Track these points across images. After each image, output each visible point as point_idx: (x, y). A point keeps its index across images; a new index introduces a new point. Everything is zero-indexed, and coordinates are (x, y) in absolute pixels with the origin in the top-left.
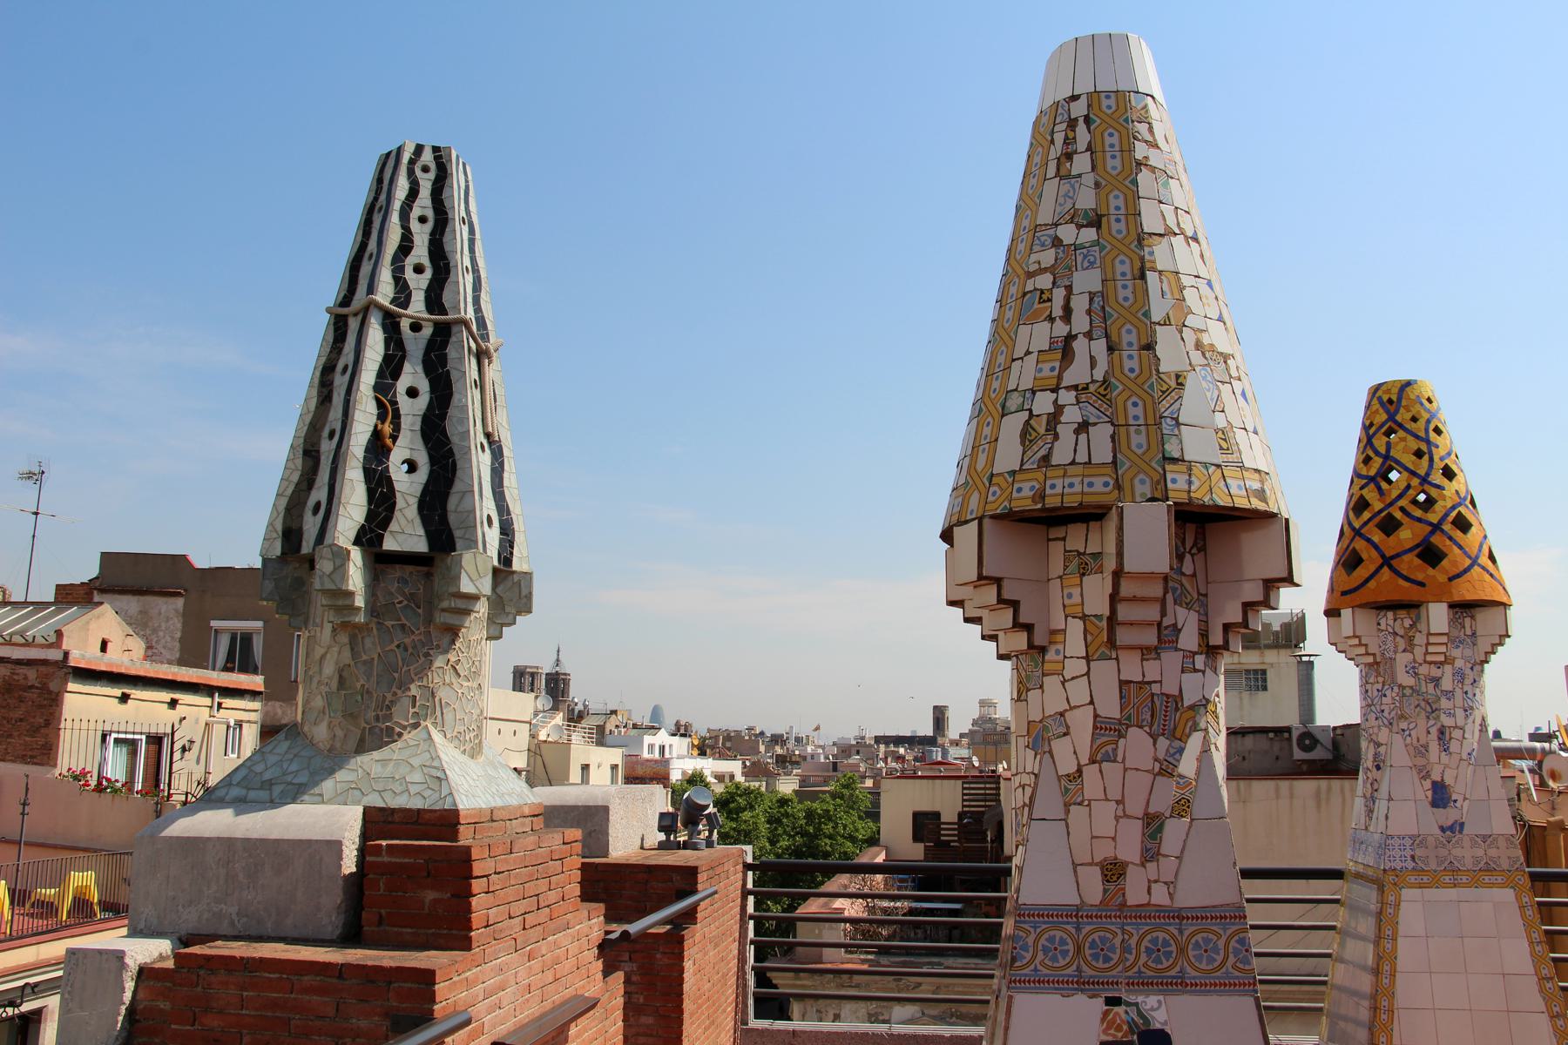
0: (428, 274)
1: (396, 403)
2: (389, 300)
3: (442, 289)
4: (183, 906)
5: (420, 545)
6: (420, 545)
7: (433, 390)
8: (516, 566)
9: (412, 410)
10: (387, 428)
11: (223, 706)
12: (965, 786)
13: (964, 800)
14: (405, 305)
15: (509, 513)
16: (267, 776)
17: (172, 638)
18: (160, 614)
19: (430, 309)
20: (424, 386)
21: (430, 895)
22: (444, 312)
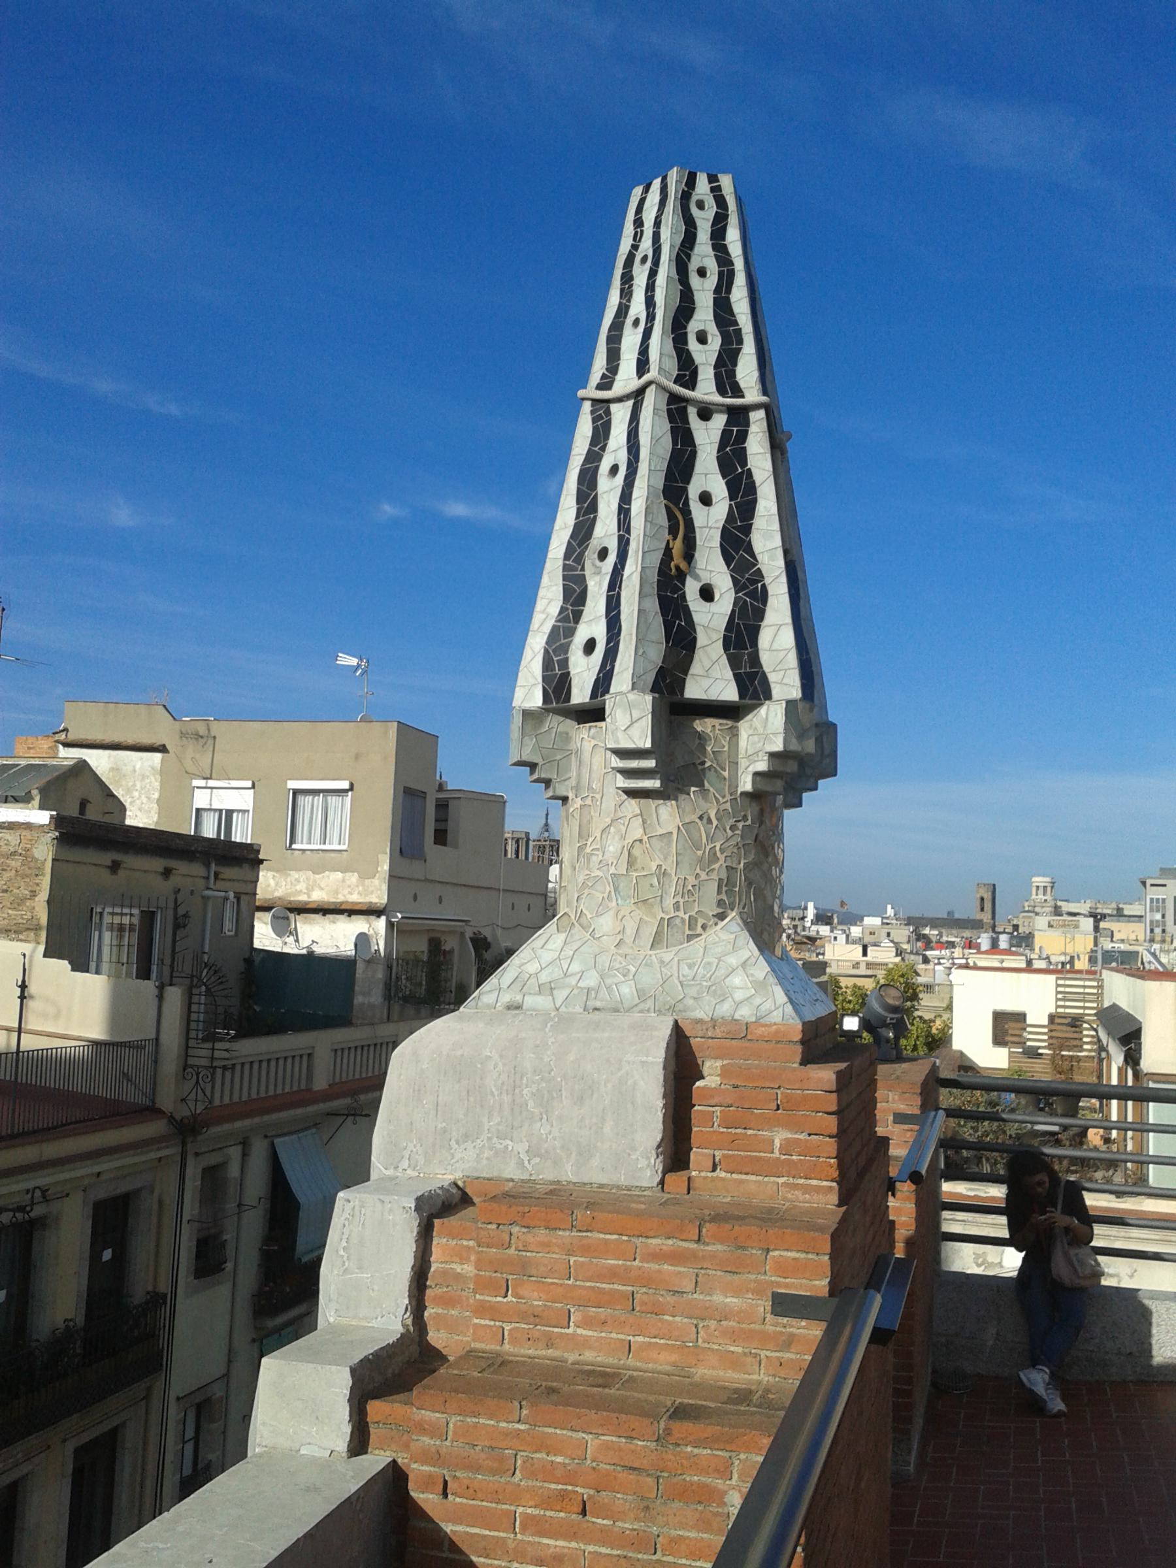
1: (690, 512)
3: (735, 365)
4: (457, 1142)
5: (729, 693)
11: (221, 876)
12: (1060, 982)
13: (1057, 1000)
14: (691, 383)
15: (807, 653)
16: (544, 977)
17: (149, 798)
18: (135, 771)
19: (721, 390)
20: (718, 488)
21: (779, 1137)
22: (737, 392)
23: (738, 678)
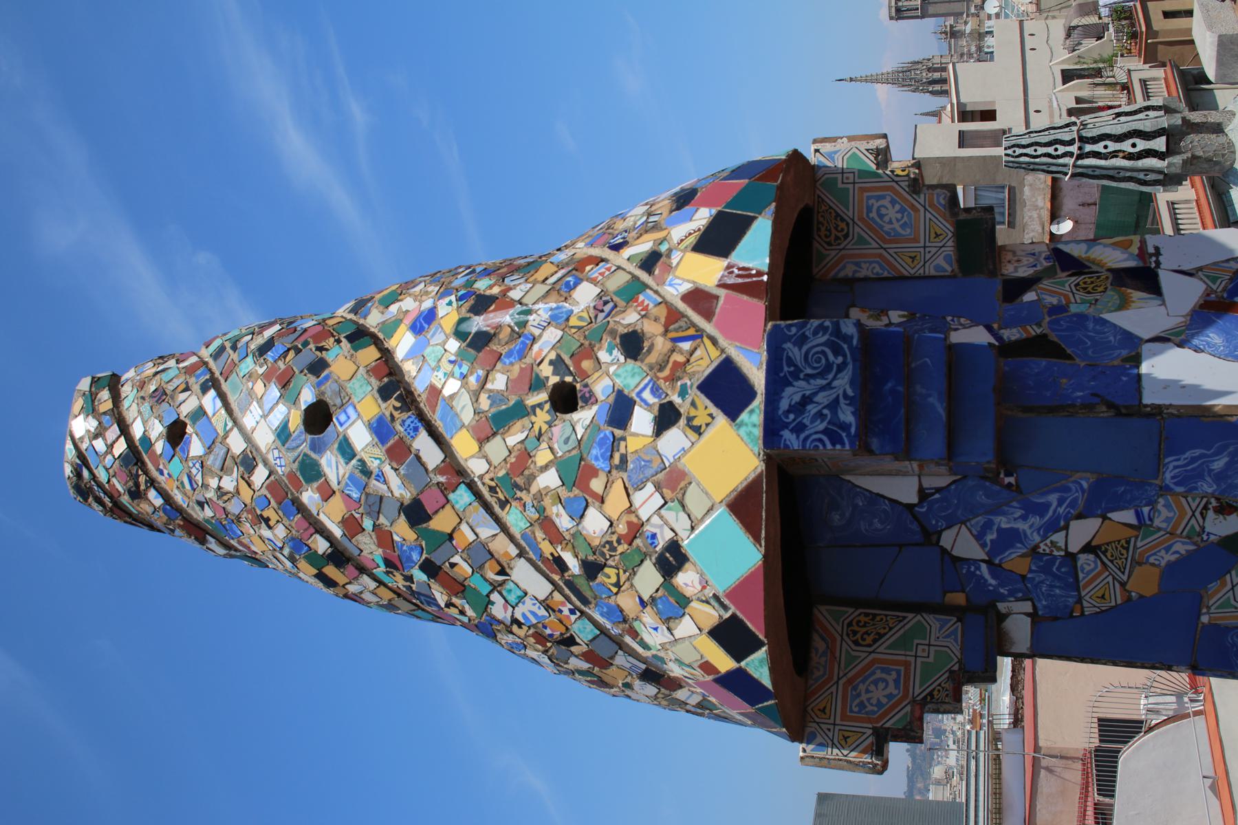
0: (1057, 146)
5: (1164, 138)
6: (1164, 138)
7: (1104, 140)
8: (1161, 104)
9: (1112, 146)
19: (1072, 144)
20: (1103, 144)
22: (1074, 139)
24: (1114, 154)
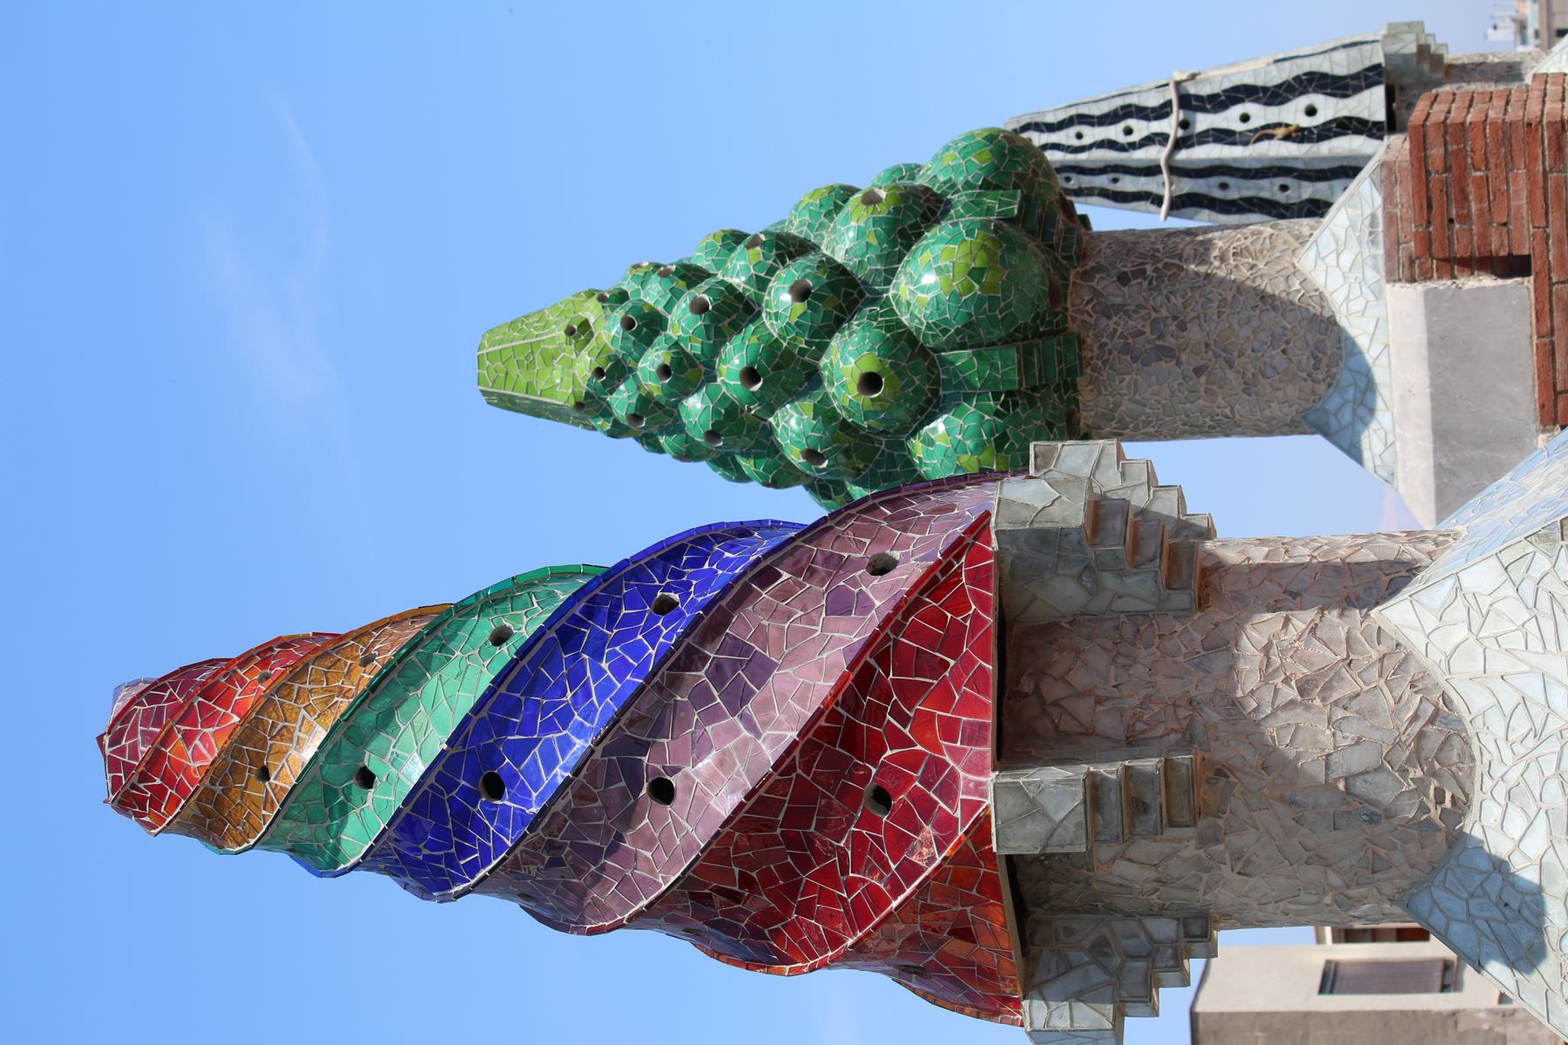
2: (1162, 148)
5: (1378, 93)
6: (1378, 93)
7: (1240, 101)
9: (1260, 115)
10: (1280, 132)
22: (1168, 104)
23: (1370, 85)
24: (1265, 133)
